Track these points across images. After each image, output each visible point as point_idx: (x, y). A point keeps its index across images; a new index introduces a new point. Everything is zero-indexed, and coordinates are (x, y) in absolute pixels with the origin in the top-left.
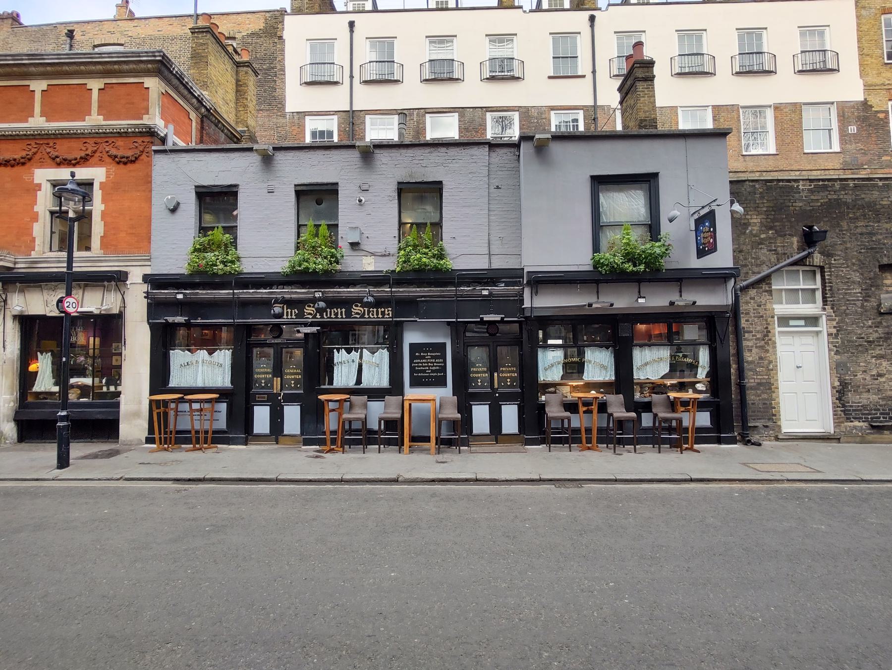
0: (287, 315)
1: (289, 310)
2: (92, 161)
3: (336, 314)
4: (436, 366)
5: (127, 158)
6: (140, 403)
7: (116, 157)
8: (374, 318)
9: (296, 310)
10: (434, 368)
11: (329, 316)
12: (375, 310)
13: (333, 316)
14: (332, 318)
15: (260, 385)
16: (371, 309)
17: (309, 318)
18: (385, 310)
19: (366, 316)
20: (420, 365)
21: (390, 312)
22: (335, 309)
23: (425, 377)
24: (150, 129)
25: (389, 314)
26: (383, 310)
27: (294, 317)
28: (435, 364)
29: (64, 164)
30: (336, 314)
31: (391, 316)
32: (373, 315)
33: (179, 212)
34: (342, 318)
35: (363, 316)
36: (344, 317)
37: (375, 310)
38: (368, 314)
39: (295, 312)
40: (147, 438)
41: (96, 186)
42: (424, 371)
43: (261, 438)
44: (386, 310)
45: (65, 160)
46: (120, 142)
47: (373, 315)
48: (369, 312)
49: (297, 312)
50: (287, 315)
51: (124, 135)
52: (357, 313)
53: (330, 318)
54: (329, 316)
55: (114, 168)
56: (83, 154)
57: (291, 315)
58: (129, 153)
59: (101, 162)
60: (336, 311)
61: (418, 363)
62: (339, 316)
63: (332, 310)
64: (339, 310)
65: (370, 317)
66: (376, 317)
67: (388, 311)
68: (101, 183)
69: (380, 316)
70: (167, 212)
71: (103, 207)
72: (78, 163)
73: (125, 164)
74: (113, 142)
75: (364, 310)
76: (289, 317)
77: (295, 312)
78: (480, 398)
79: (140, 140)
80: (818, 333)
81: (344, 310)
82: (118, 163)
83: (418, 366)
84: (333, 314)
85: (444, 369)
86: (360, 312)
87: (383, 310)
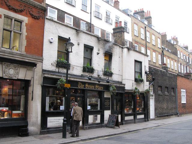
2: (23, 13)
3: (92, 88)
5: (36, 17)
7: (33, 15)
23: (107, 107)
29: (12, 10)
30: (92, 88)
33: (52, 43)
35: (97, 89)
40: (41, 132)
41: (24, 24)
45: (13, 8)
46: (34, 10)
51: (36, 7)
55: (31, 19)
56: (21, 9)
58: (37, 15)
59: (25, 15)
68: (26, 24)
70: (50, 43)
71: (26, 34)
72: (18, 12)
73: (35, 19)
74: (31, 9)
79: (40, 11)
80: (153, 98)
82: (33, 18)
85: (110, 104)
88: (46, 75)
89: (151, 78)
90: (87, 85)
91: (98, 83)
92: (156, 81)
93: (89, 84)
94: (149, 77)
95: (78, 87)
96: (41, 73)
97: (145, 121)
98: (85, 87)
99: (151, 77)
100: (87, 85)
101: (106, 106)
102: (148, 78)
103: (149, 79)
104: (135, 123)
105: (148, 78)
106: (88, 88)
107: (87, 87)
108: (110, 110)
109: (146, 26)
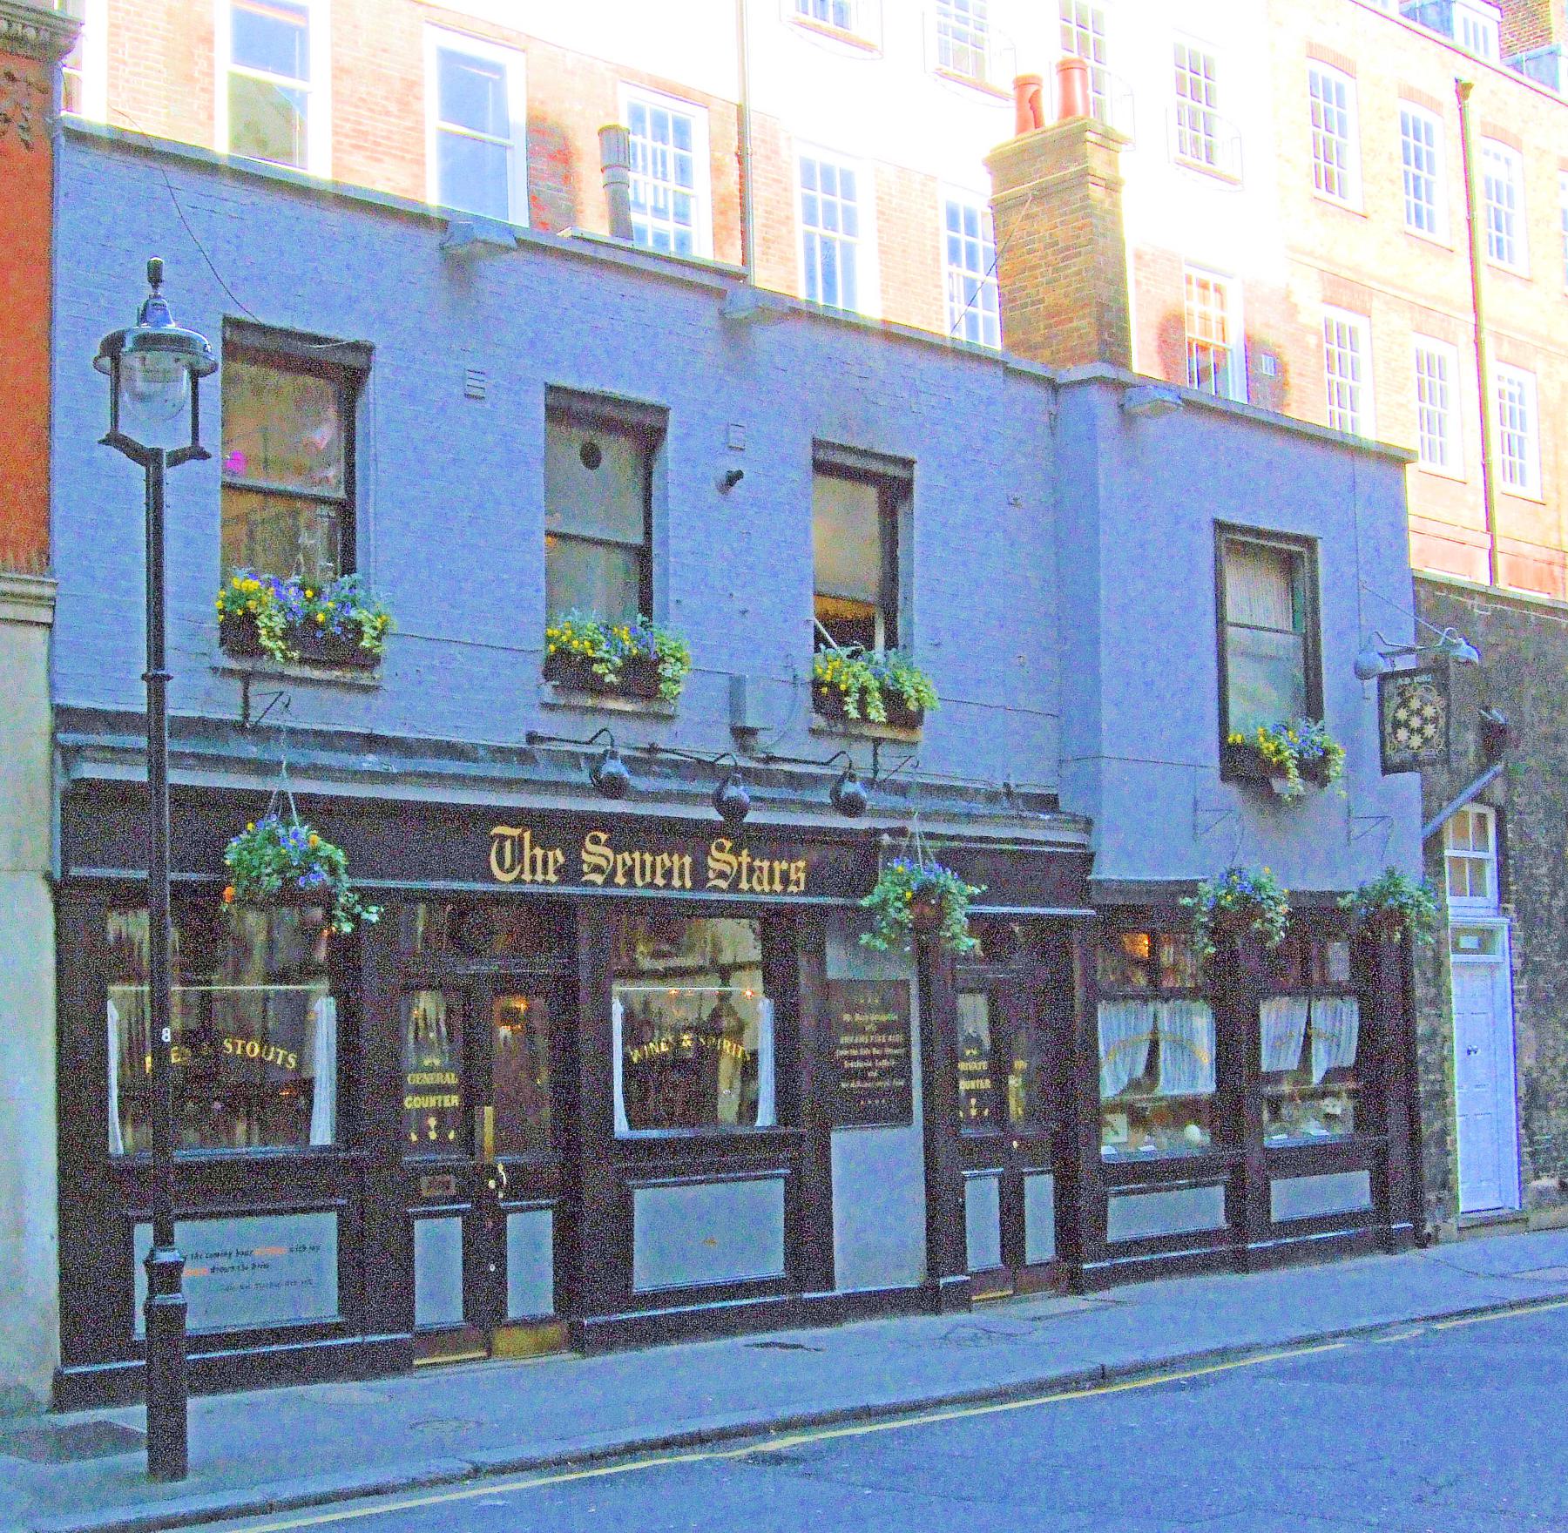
0: (533, 871)
1: (539, 852)
3: (668, 874)
4: (889, 1057)
6: (19, 1228)
8: (773, 892)
9: (558, 852)
10: (885, 1063)
11: (648, 879)
12: (766, 864)
13: (660, 881)
14: (657, 887)
15: (423, 1134)
16: (757, 863)
17: (593, 884)
18: (789, 868)
19: (744, 885)
20: (855, 1052)
21: (802, 876)
22: (665, 856)
23: (870, 1094)
24: (53, 34)
25: (797, 883)
26: (784, 866)
27: (552, 878)
28: (888, 1051)
30: (668, 874)
31: (802, 887)
32: (760, 882)
34: (683, 887)
35: (734, 887)
36: (688, 884)
37: (766, 864)
38: (749, 881)
39: (556, 861)
40: (59, 1380)
42: (862, 1075)
43: (435, 1339)
44: (793, 865)
47: (760, 882)
48: (751, 870)
49: (561, 860)
50: (533, 871)
52: (722, 875)
53: (651, 885)
54: (648, 879)
57: (545, 872)
60: (668, 864)
61: (849, 1047)
62: (676, 883)
63: (658, 859)
64: (676, 857)
65: (752, 890)
66: (767, 889)
67: (798, 869)
69: (778, 887)
75: (740, 864)
76: (539, 877)
77: (556, 861)
78: (978, 1154)
80: (1493, 967)
81: (687, 860)
83: (850, 1058)
84: (659, 871)
86: (729, 872)
87: (784, 866)
88: (89, 771)
89: (1429, 730)
90: (595, 853)
91: (713, 815)
92: (1527, 756)
93: (625, 832)
94: (1415, 722)
95: (493, 880)
96: (40, 750)
97: (1387, 1243)
98: (571, 872)
99: (1429, 712)
100: (595, 853)
101: (851, 1075)
102: (1397, 724)
103: (1416, 741)
104: (1242, 1262)
105: (1397, 724)
106: (610, 881)
107: (597, 869)
108: (902, 1115)
109: (1467, 73)
